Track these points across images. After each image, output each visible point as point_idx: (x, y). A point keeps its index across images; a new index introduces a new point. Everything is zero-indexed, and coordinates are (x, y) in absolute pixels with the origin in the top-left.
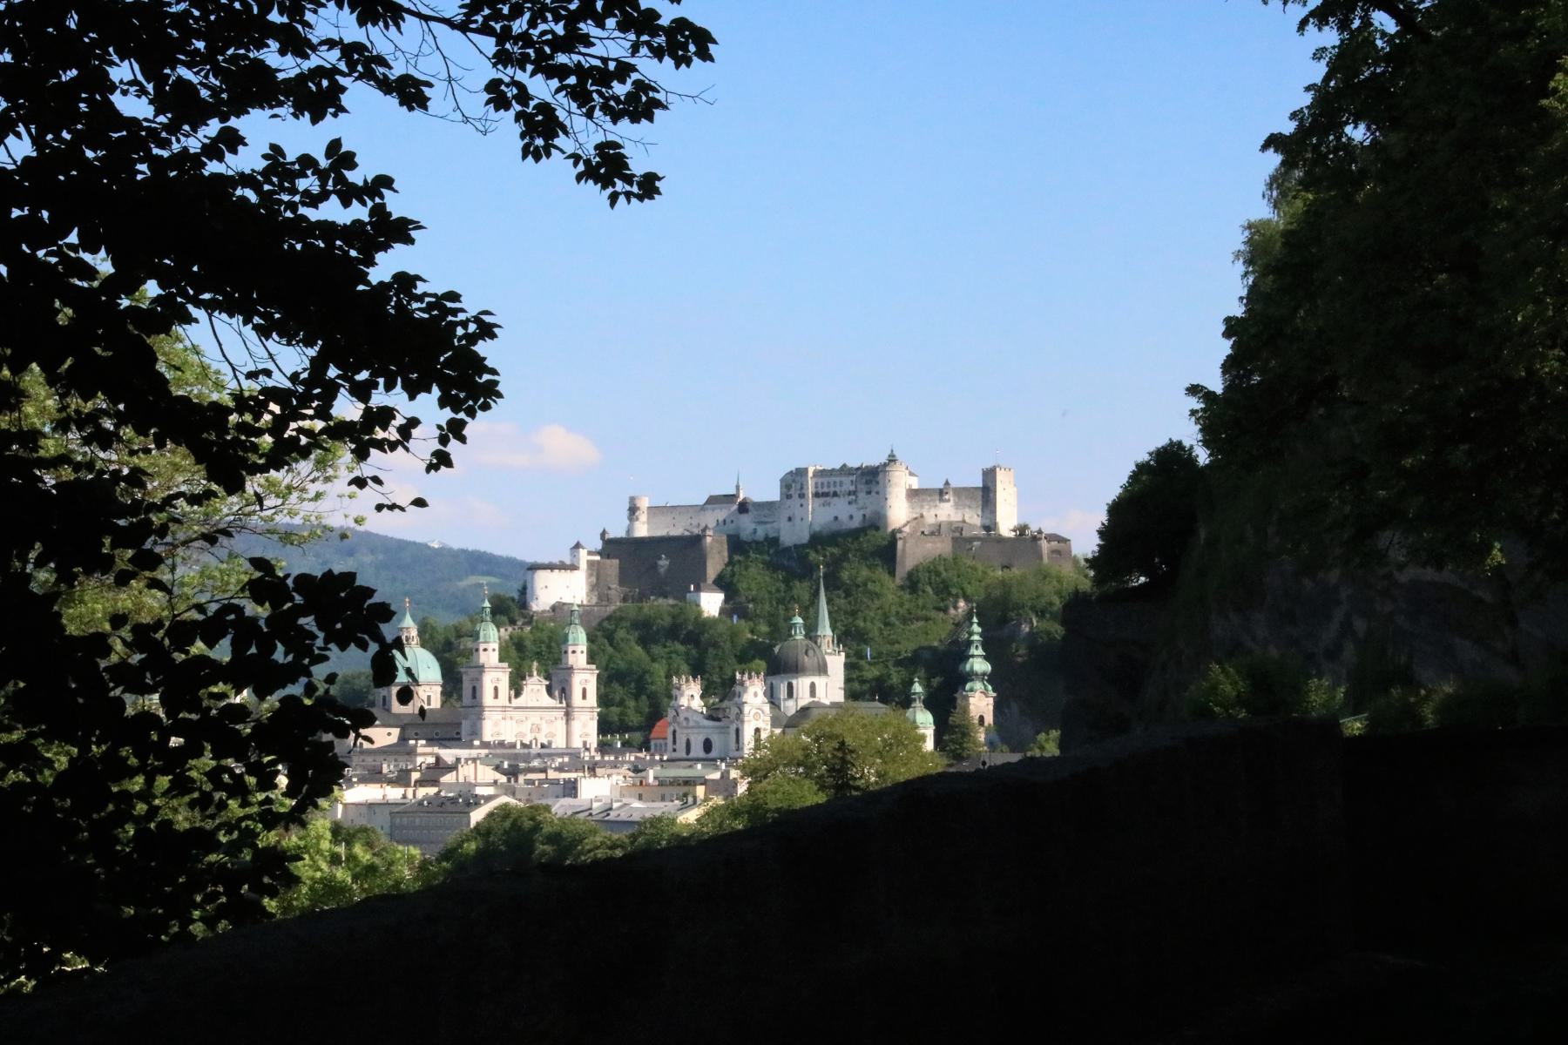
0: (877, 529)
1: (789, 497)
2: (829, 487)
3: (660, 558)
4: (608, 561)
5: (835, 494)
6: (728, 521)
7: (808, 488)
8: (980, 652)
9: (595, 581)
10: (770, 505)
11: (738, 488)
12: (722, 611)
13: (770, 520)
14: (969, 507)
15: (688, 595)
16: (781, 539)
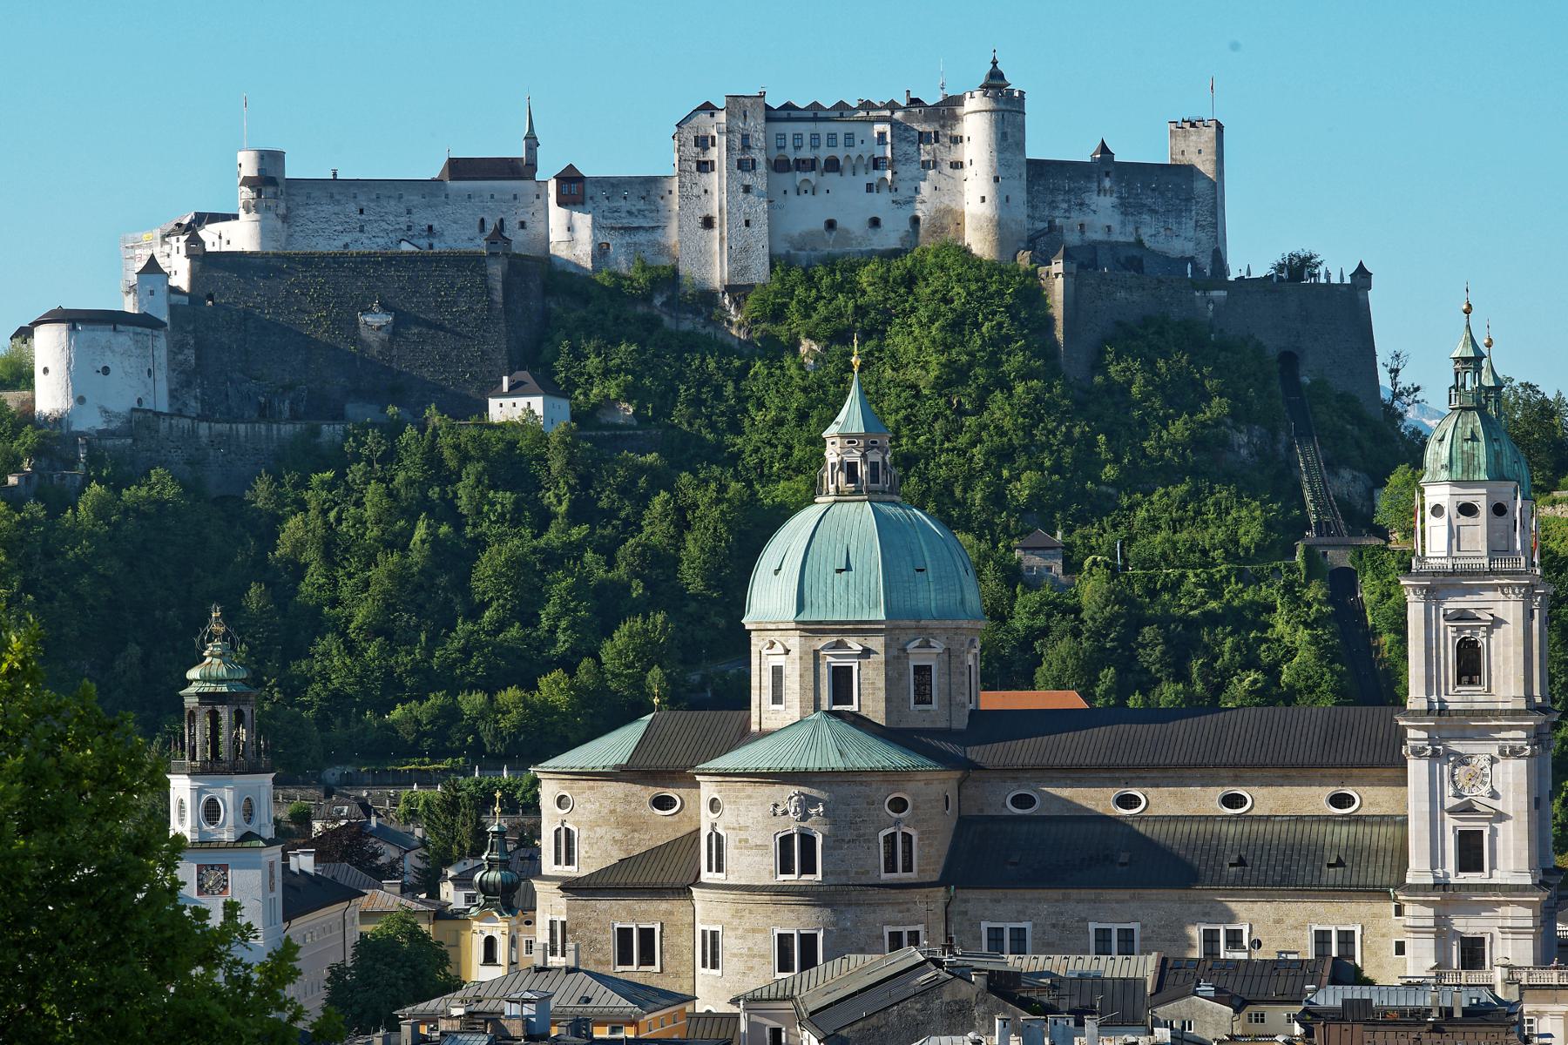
1: (704, 167)
2: (815, 147)
3: (368, 311)
5: (833, 165)
11: (532, 142)
14: (1152, 211)
16: (684, 269)
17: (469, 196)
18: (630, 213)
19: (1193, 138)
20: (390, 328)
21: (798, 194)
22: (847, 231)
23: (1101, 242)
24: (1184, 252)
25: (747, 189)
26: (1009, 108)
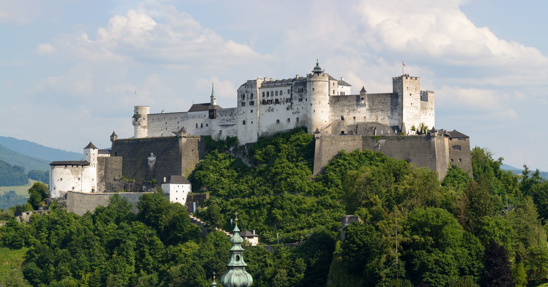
0: (306, 130)
1: (243, 104)
2: (272, 95)
3: (150, 156)
4: (114, 158)
5: (277, 102)
6: (204, 125)
7: (256, 98)
8: (242, 263)
9: (103, 174)
10: (231, 111)
11: (212, 97)
12: (189, 198)
13: (231, 124)
14: (382, 110)
15: (163, 185)
16: (239, 138)
17: (193, 117)
18: (227, 120)
19: (398, 83)
20: (155, 161)
21: (269, 112)
22: (282, 123)
23: (361, 123)
24: (394, 124)
25: (252, 111)
26: (315, 80)
